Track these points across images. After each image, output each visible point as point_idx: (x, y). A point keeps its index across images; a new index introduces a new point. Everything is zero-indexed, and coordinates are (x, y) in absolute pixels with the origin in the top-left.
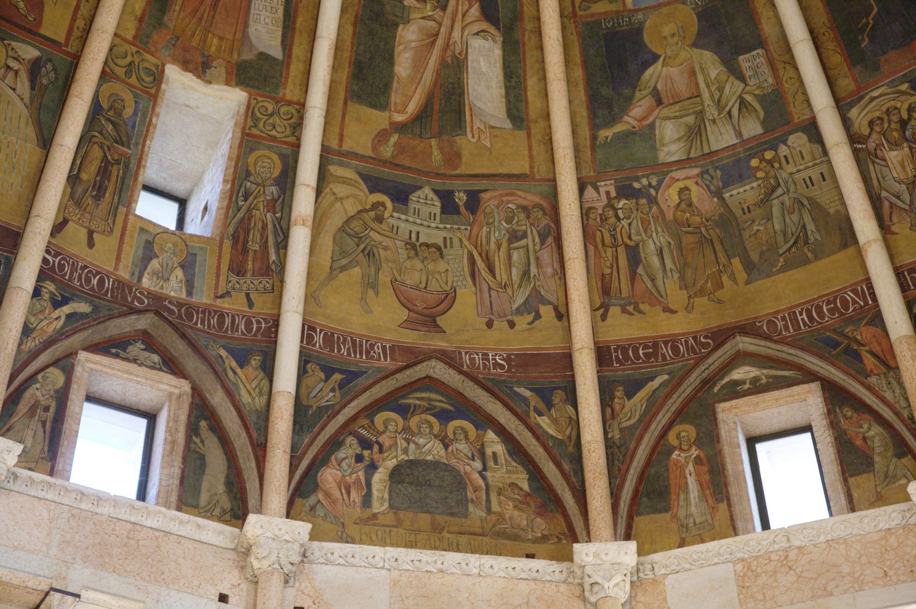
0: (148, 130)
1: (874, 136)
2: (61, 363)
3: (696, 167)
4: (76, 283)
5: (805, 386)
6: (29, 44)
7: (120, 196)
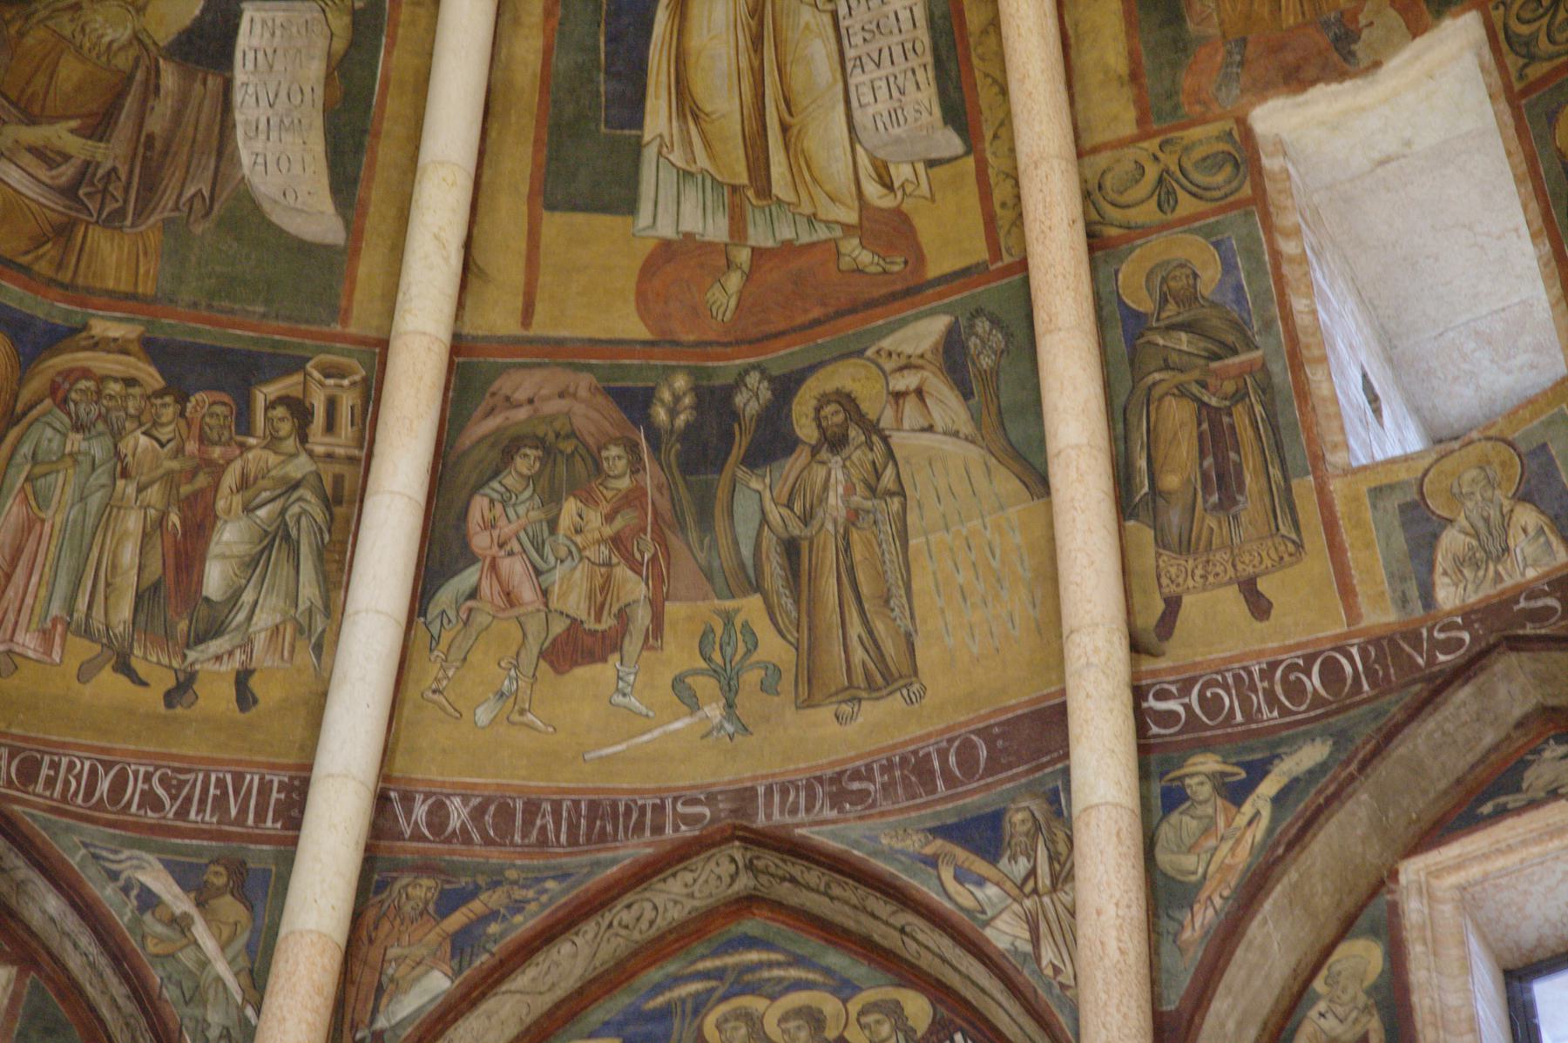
0: (1279, 279)
2: (1363, 921)
4: (1270, 716)
6: (917, 317)
7: (1283, 462)
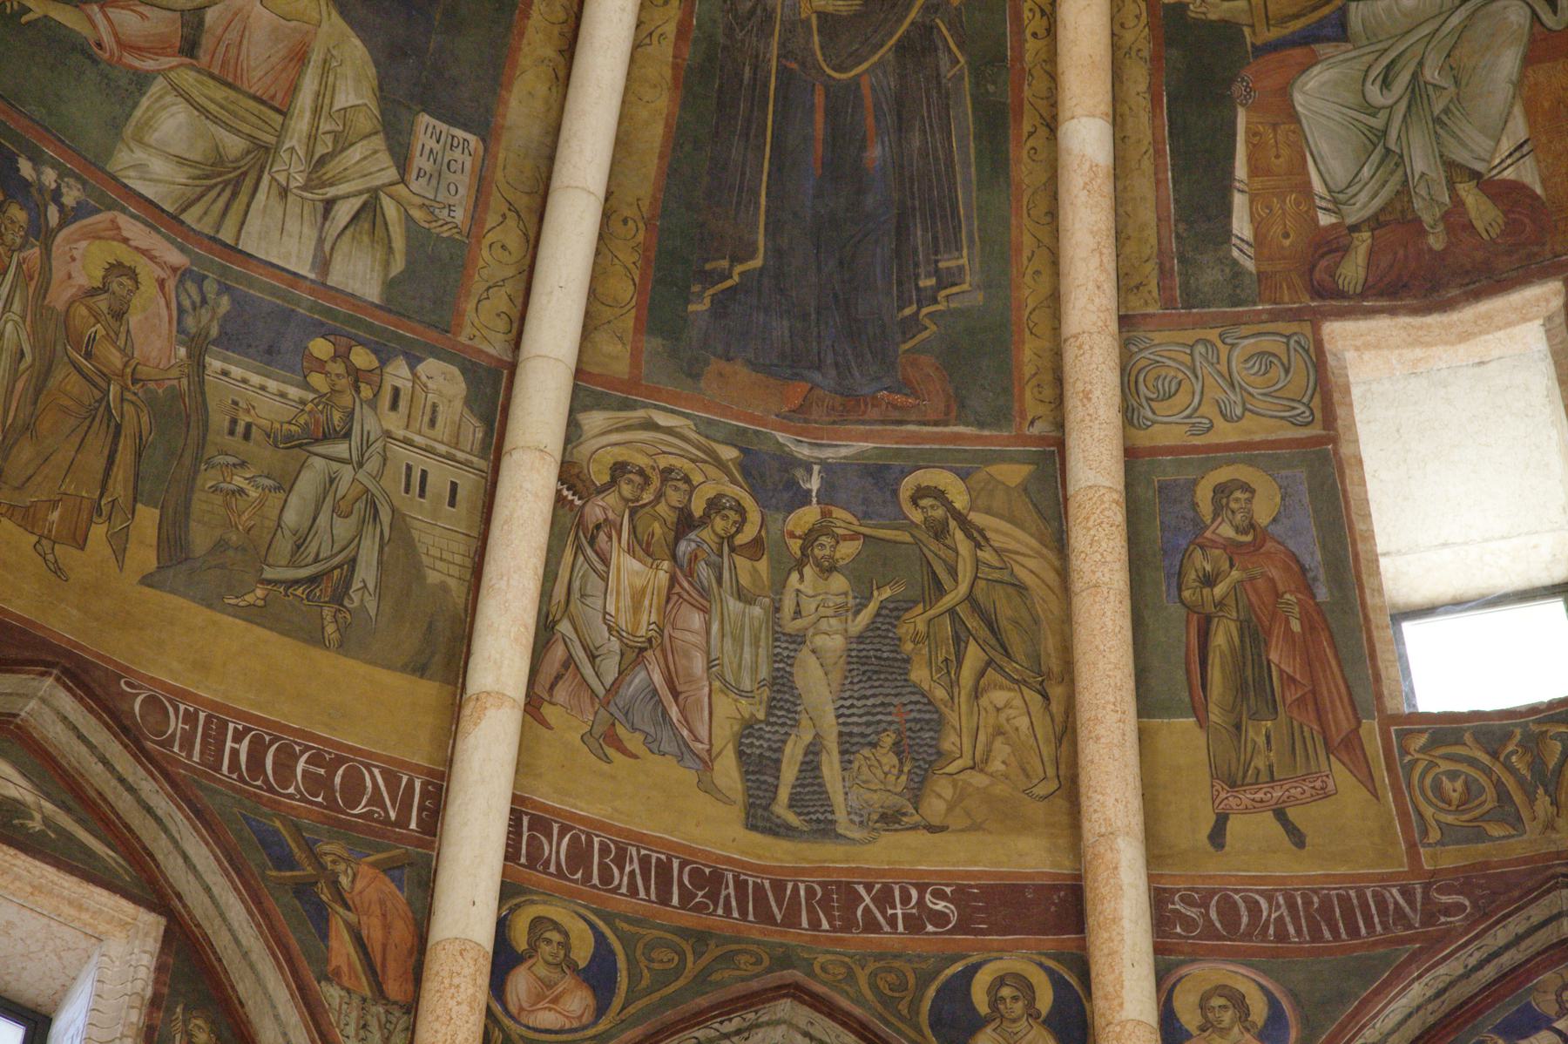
1: (611, 499)
3: (182, 249)
5: (128, 907)
